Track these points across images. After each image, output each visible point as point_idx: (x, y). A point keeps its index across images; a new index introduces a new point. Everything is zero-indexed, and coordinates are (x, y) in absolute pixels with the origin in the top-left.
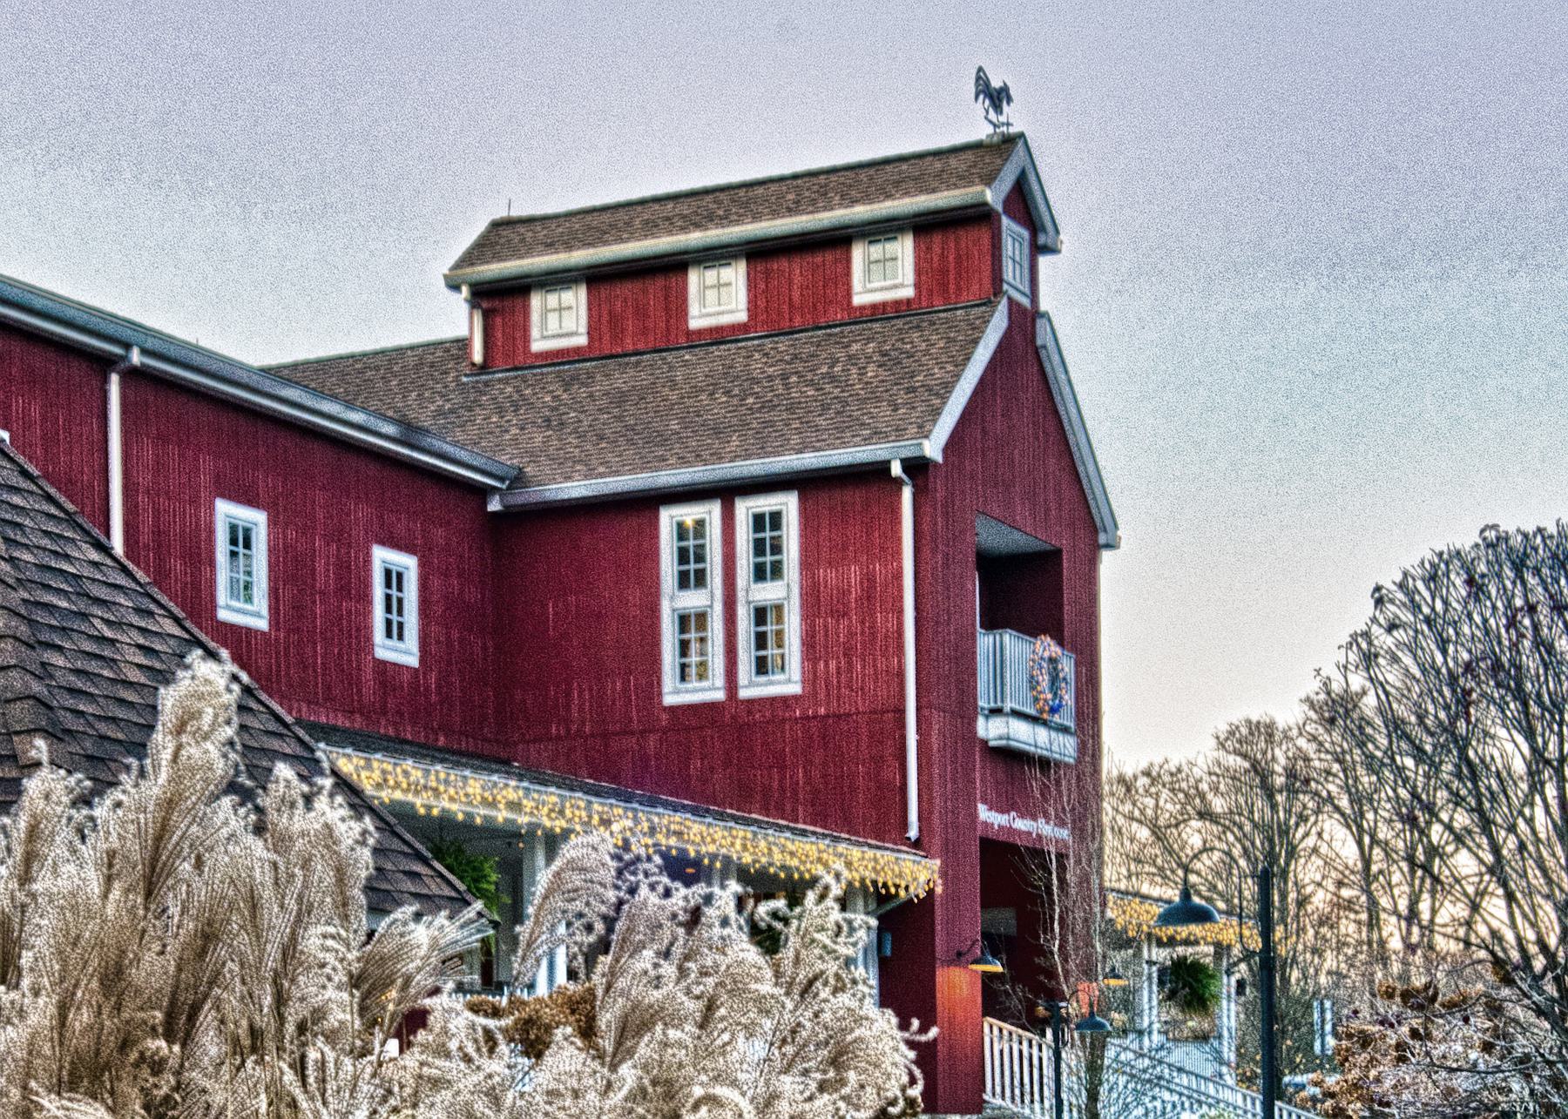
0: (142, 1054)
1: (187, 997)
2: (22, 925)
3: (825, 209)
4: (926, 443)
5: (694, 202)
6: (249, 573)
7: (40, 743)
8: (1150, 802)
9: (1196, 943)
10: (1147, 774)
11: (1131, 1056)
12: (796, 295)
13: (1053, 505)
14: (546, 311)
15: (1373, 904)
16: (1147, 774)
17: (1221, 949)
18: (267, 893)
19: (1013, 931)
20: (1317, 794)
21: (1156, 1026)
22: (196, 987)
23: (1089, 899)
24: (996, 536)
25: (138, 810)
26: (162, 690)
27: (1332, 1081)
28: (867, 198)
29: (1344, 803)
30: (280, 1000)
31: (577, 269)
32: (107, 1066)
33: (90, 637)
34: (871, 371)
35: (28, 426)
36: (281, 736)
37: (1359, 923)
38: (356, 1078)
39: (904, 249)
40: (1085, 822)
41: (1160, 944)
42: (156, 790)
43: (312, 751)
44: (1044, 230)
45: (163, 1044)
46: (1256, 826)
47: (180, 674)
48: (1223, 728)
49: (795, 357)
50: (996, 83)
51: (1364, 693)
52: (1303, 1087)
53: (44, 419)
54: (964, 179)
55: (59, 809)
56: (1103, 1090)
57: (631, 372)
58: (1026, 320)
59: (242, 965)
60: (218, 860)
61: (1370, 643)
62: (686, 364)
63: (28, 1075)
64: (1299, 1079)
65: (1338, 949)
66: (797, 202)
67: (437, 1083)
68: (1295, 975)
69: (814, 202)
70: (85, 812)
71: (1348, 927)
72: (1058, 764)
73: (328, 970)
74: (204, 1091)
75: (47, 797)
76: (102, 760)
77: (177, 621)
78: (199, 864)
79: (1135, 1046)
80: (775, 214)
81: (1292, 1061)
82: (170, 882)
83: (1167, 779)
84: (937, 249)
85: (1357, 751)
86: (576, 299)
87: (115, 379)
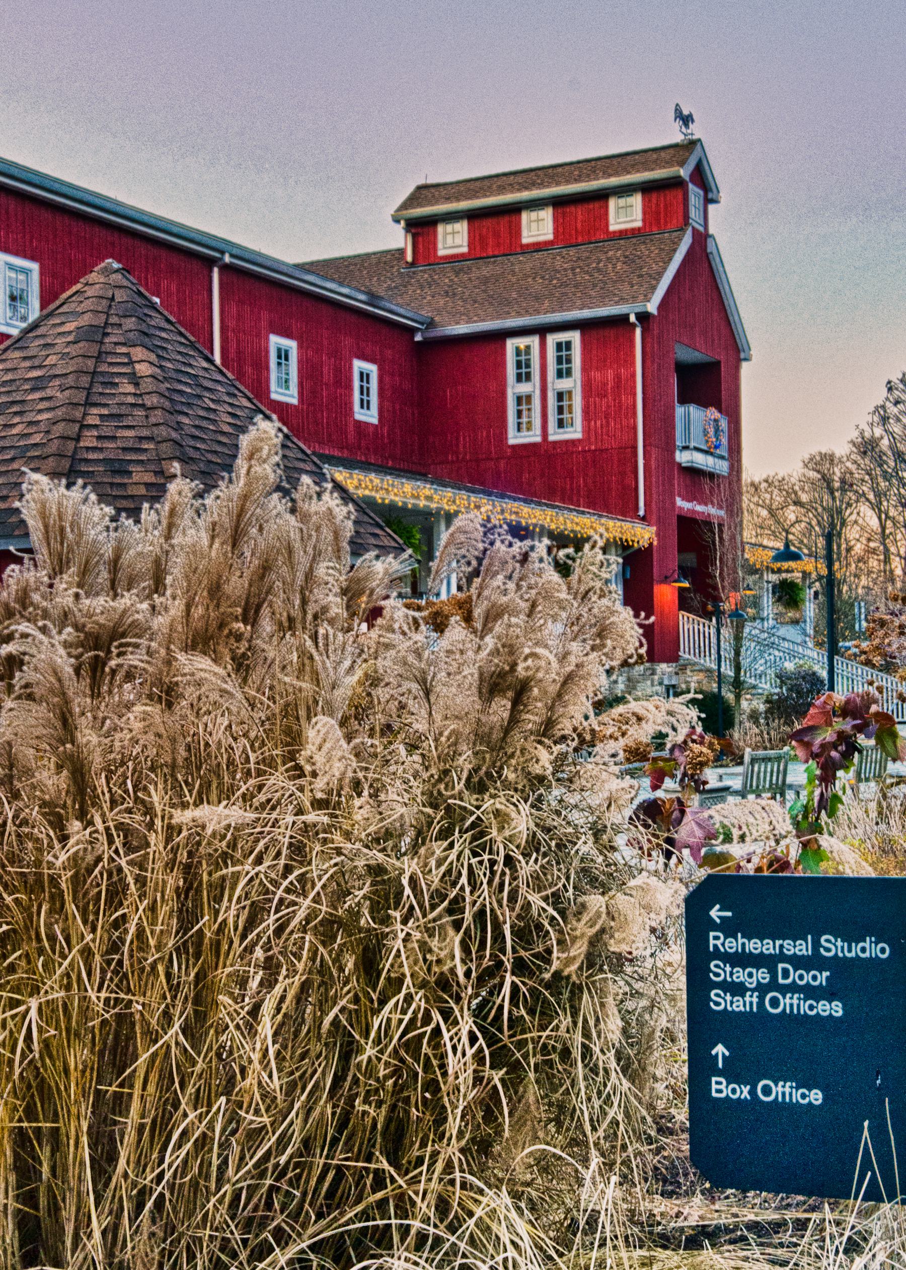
0: (230, 630)
1: (254, 600)
2: (166, 562)
3: (595, 179)
4: (648, 305)
5: (525, 176)
6: (287, 374)
7: (176, 465)
8: (768, 496)
9: (792, 571)
10: (766, 481)
11: (757, 631)
12: (579, 225)
13: (716, 338)
14: (446, 234)
15: (887, 551)
16: (766, 481)
17: (806, 575)
18: (297, 545)
19: (695, 565)
20: (857, 492)
21: (771, 616)
22: (259, 595)
23: (735, 548)
24: (685, 354)
25: (228, 500)
26: (241, 437)
27: (865, 645)
28: (617, 174)
29: (871, 496)
30: (304, 602)
31: (462, 211)
32: (212, 637)
33: (203, 408)
34: (619, 266)
35: (169, 295)
36: (304, 461)
37: (879, 560)
38: (344, 643)
39: (637, 200)
40: (733, 507)
41: (773, 572)
42: (238, 490)
43: (321, 469)
44: (711, 191)
45: (242, 625)
46: (824, 509)
47: (251, 428)
48: (807, 457)
49: (579, 258)
50: (686, 112)
51: (882, 438)
52: (849, 648)
53: (178, 291)
54: (668, 163)
55: (186, 500)
56: (743, 650)
57: (491, 267)
58: (702, 239)
59: (284, 583)
60: (271, 527)
61: (885, 411)
62: (520, 262)
63: (170, 642)
64: (847, 644)
65: (868, 575)
66: (580, 176)
67: (387, 646)
68: (845, 588)
69: (588, 176)
70: (200, 501)
71: (873, 563)
72: (719, 476)
73: (329, 586)
74: (263, 650)
75: (180, 493)
76: (209, 473)
77: (249, 399)
78: (261, 529)
79: (760, 626)
80: (568, 182)
81: (843, 635)
82: (245, 539)
83: (777, 484)
84: (654, 201)
85: (878, 469)
86: (462, 228)
87: (216, 271)
